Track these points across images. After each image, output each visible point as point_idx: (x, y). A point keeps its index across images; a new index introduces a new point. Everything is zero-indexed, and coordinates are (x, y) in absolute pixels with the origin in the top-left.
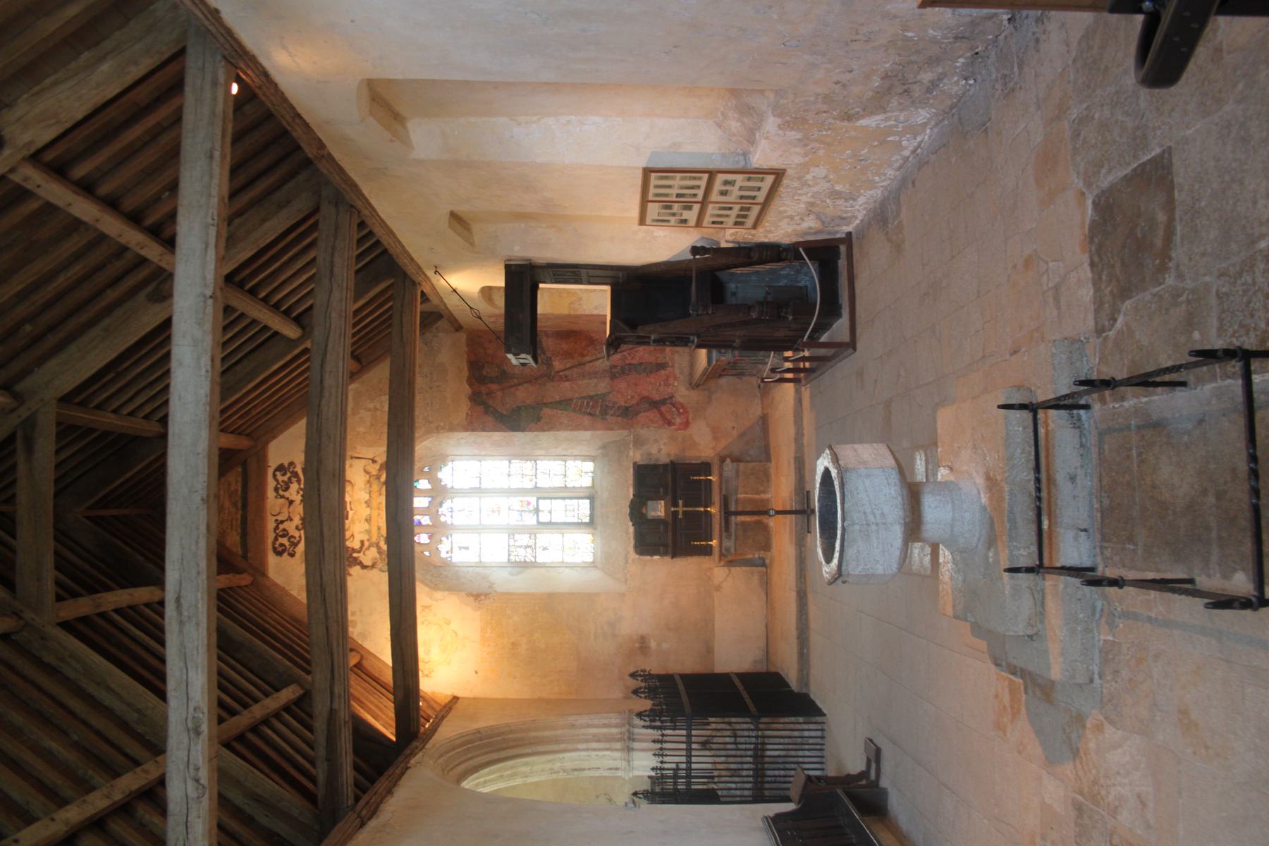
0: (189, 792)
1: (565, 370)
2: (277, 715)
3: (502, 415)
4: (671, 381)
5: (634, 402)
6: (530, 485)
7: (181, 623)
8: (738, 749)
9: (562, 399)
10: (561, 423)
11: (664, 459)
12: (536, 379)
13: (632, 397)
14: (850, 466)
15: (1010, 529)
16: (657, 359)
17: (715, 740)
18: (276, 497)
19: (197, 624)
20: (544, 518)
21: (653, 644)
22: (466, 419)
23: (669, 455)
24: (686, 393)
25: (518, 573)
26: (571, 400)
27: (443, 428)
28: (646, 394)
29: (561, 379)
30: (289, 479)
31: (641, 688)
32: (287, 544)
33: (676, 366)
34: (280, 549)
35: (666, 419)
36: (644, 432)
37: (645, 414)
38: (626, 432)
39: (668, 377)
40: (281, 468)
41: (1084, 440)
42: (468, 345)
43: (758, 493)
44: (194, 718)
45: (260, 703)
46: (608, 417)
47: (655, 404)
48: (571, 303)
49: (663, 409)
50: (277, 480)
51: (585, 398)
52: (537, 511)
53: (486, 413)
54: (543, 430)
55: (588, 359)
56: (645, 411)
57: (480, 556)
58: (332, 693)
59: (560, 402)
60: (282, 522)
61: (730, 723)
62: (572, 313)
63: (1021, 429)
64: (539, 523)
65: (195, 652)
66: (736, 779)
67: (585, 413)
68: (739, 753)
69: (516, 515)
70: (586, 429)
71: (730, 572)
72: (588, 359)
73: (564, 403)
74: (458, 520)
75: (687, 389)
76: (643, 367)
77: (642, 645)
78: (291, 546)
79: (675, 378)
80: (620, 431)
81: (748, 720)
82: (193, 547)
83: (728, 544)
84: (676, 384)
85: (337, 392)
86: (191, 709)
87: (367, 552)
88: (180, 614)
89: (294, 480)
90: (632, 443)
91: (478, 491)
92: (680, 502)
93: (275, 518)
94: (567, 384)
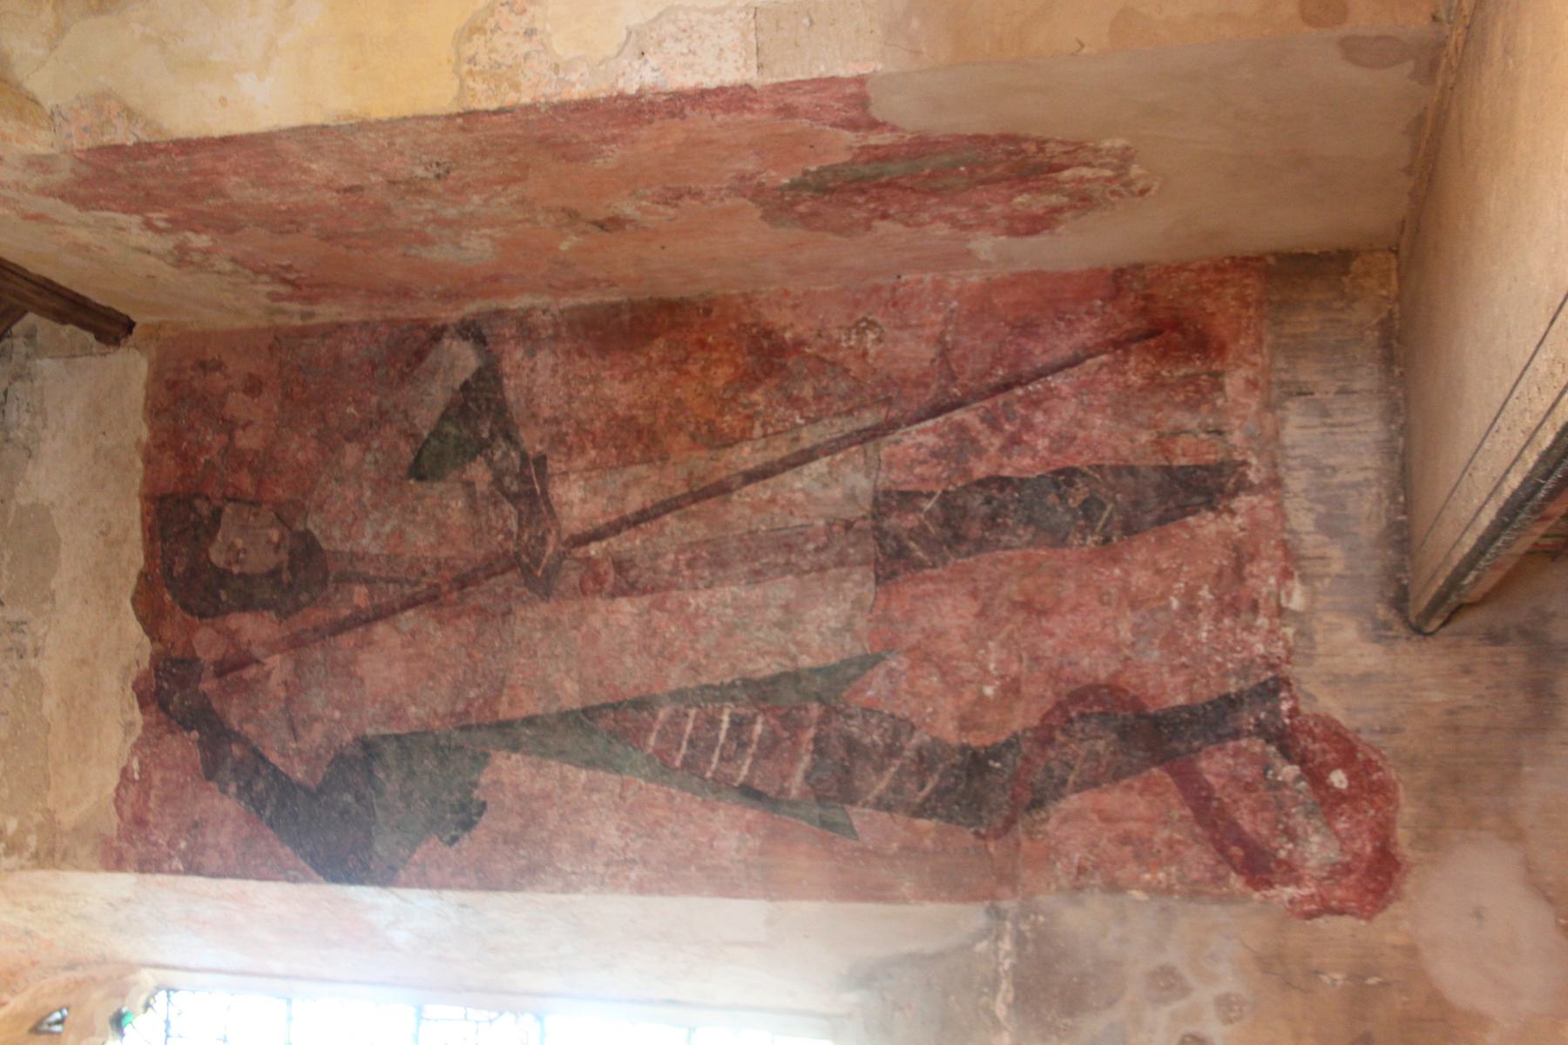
1: (615, 528)
3: (284, 786)
4: (1263, 578)
5: (1022, 718)
9: (600, 697)
10: (588, 845)
12: (462, 582)
13: (1012, 688)
16: (1162, 443)
22: (118, 800)
24: (1370, 657)
26: (642, 704)
28: (1095, 665)
29: (593, 582)
33: (1297, 481)
35: (1242, 840)
38: (973, 916)
39: (1241, 556)
42: (154, 411)
46: (858, 816)
48: (474, 29)
49: (1214, 766)
51: (723, 692)
53: (211, 770)
54: (488, 882)
55: (747, 456)
56: (1080, 787)
59: (584, 718)
62: (485, 101)
67: (720, 785)
70: (728, 888)
72: (747, 456)
75: (1379, 633)
76: (1080, 492)
80: (930, 908)
84: (1297, 600)
90: (1006, 990)
94: (626, 607)
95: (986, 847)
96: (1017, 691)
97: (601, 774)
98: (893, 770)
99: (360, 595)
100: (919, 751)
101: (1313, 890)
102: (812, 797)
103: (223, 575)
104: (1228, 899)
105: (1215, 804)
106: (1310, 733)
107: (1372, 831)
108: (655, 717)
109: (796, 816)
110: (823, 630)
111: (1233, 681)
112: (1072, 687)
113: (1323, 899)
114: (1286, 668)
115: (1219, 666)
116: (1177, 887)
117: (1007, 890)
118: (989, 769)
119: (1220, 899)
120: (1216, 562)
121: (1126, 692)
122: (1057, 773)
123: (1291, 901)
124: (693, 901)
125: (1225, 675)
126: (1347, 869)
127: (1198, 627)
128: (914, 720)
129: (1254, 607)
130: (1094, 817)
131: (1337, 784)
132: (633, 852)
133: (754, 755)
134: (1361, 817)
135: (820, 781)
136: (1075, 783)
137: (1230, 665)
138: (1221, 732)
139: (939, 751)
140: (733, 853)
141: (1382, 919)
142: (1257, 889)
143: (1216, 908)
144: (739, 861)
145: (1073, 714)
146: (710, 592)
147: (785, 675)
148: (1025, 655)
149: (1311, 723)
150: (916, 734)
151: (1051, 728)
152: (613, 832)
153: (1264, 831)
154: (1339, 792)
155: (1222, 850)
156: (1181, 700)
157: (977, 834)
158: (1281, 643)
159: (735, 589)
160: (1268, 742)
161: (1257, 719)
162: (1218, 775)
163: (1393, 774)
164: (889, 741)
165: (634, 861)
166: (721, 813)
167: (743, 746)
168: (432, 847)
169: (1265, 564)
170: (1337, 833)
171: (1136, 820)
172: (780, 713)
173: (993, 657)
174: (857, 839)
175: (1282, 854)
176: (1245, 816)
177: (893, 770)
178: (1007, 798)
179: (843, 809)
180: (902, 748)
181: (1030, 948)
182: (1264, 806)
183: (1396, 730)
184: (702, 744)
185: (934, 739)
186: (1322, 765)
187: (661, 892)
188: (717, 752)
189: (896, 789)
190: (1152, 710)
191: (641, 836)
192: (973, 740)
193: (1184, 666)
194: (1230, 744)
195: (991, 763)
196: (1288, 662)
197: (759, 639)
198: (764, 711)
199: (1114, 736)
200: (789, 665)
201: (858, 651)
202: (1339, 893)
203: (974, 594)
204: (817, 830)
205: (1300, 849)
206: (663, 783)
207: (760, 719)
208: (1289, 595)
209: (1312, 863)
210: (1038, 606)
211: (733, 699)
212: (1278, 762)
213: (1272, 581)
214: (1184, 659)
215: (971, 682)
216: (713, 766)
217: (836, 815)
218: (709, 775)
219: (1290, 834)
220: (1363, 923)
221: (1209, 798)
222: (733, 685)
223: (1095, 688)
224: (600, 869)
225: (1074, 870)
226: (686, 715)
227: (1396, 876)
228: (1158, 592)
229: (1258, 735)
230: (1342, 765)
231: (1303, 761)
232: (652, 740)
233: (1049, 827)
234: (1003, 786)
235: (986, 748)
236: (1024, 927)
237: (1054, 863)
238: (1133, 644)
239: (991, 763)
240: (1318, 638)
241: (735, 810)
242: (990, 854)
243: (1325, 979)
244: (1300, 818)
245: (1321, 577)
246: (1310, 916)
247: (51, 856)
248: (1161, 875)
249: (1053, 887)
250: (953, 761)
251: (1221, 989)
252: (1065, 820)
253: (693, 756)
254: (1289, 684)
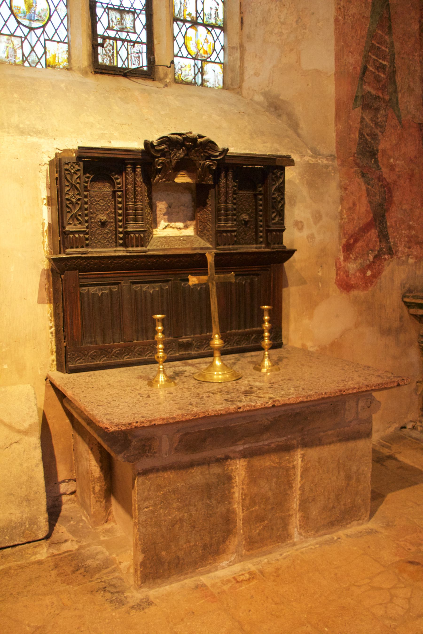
13: (392, 168)
24: (397, 282)
28: (397, 196)
35: (356, 241)
37: (364, 193)
46: (359, 109)
49: (373, 234)
51: (392, 63)
56: (367, 189)
67: (366, 58)
70: (338, 58)
71: (26, 433)
75: (403, 285)
83: (165, 446)
92: (231, 277)
95: (351, 156)
96: (391, 170)
97: (370, 9)
98: (372, 125)
100: (376, 135)
101: (342, 265)
102: (363, 94)
104: (340, 239)
105: (363, 234)
106: (380, 264)
107: (357, 283)
108: (386, 34)
109: (358, 87)
110: (408, 103)
111: (393, 241)
112: (392, 188)
113: (340, 268)
114: (395, 257)
115: (396, 236)
116: (342, 222)
117: (340, 163)
118: (371, 159)
119: (340, 235)
120: (420, 236)
121: (390, 207)
122: (371, 182)
123: (339, 258)
124: (333, 42)
125: (394, 238)
126: (347, 276)
127: (405, 230)
128: (384, 133)
129: (409, 248)
130: (360, 194)
131: (368, 273)
132: (347, 19)
133: (375, 72)
134: (360, 280)
135: (368, 98)
136: (368, 188)
137: (396, 240)
138: (381, 236)
139: (377, 142)
140: (348, 61)
141: (335, 286)
142: (343, 247)
143: (338, 234)
144: (346, 63)
145: (385, 189)
146: (419, 62)
147: (396, 88)
148: (400, 173)
149: (382, 265)
150: (381, 134)
151: (382, 182)
152: (354, 11)
153: (357, 250)
154: (366, 273)
155: (352, 236)
156: (388, 224)
157: (355, 153)
158: (401, 255)
159: (419, 71)
160: (378, 251)
161: (384, 248)
162: (370, 235)
163: (370, 290)
164: (379, 124)
165: (344, 18)
166: (359, 58)
167: (378, 69)
169: (419, 251)
170: (356, 272)
171: (359, 208)
172: (386, 84)
173: (400, 162)
174: (353, 109)
175: (351, 256)
176: (361, 244)
177: (372, 125)
178: (365, 165)
179: (360, 105)
180: (377, 128)
181: (324, 170)
182: (363, 250)
183: (380, 290)
184: (378, 53)
185: (379, 140)
186: (372, 268)
187: (336, 29)
188: (376, 58)
189: (367, 126)
190: (386, 214)
191: (352, 23)
192: (380, 154)
193: (396, 225)
194: (378, 240)
195: (373, 160)
196: (397, 258)
197: (406, 78)
198: (387, 78)
199: (380, 202)
200: (399, 89)
201: (403, 115)
202: (342, 273)
203: (415, 157)
204: (355, 95)
205: (352, 261)
206: (368, 35)
207: (385, 76)
208: (412, 258)
209: (349, 265)
210: (412, 178)
211: (390, 66)
212: (373, 255)
213: (415, 253)
214: (398, 225)
215: (394, 154)
216: (372, 56)
217: (359, 102)
218: (370, 54)
219: (356, 259)
220: (334, 281)
221: (364, 232)
222: (394, 67)
223: (392, 197)
224: (342, 4)
225: (346, 187)
226: (386, 47)
227: (345, 291)
228: (414, 218)
229: (380, 248)
230: (371, 275)
231: (373, 262)
232: (380, 32)
233: (357, 178)
234: (367, 163)
235: (377, 158)
236: (330, 168)
237: (348, 180)
238: (402, 209)
239: (373, 160)
240: (402, 267)
241: (360, 63)
242: (349, 158)
243: (320, 269)
244: (360, 261)
245: (416, 268)
246: (336, 264)
248: (345, 216)
249: (341, 179)
250: (374, 146)
251: (316, 236)
252: (359, 184)
253: (375, 48)
254: (391, 258)
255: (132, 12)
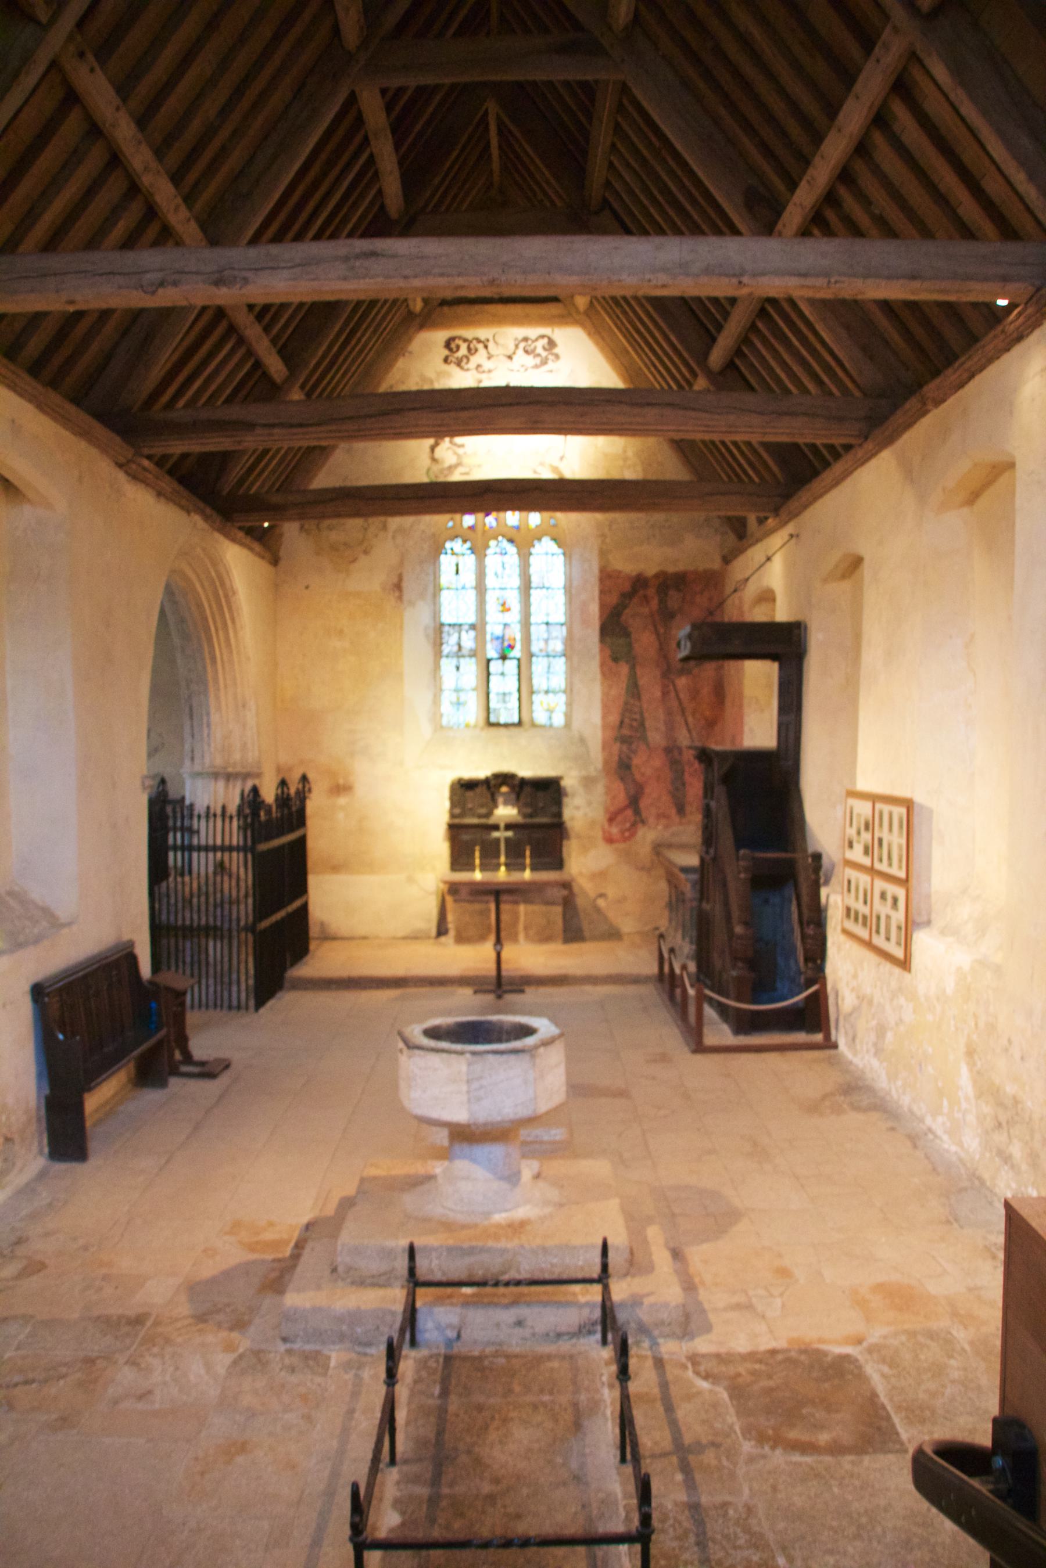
0: (148, 276)
2: (250, 353)
4: (663, 821)
5: (638, 777)
6: (535, 648)
7: (346, 259)
8: (215, 906)
11: (568, 813)
13: (643, 775)
14: (538, 1061)
15: (461, 1249)
17: (226, 878)
18: (516, 339)
19: (345, 279)
20: (495, 667)
21: (342, 801)
23: (572, 819)
25: (427, 636)
26: (639, 698)
27: (603, 542)
28: (647, 790)
30: (539, 355)
31: (288, 789)
32: (460, 354)
34: (453, 346)
36: (600, 788)
40: (552, 344)
41: (566, 1337)
42: (705, 571)
43: (526, 928)
44: (235, 277)
45: (264, 335)
46: (618, 744)
47: (634, 802)
49: (629, 812)
50: (536, 340)
52: (504, 658)
55: (690, 719)
57: (448, 588)
58: (273, 426)
60: (486, 347)
61: (246, 896)
63: (580, 1263)
64: (489, 661)
65: (312, 276)
66: (180, 905)
67: (623, 715)
68: (211, 909)
69: (498, 631)
73: (634, 690)
74: (492, 561)
77: (341, 788)
78: (457, 358)
79: (667, 827)
81: (251, 918)
82: (436, 271)
84: (660, 827)
85: (638, 424)
86: (244, 274)
87: (450, 452)
88: (357, 257)
89: (538, 361)
91: (526, 587)
93: (491, 339)
94: (658, 694)
99: (662, 631)
103: (666, 595)
168: (608, 652)
192: (634, 769)
247: (603, 553)
255: (510, 694)
